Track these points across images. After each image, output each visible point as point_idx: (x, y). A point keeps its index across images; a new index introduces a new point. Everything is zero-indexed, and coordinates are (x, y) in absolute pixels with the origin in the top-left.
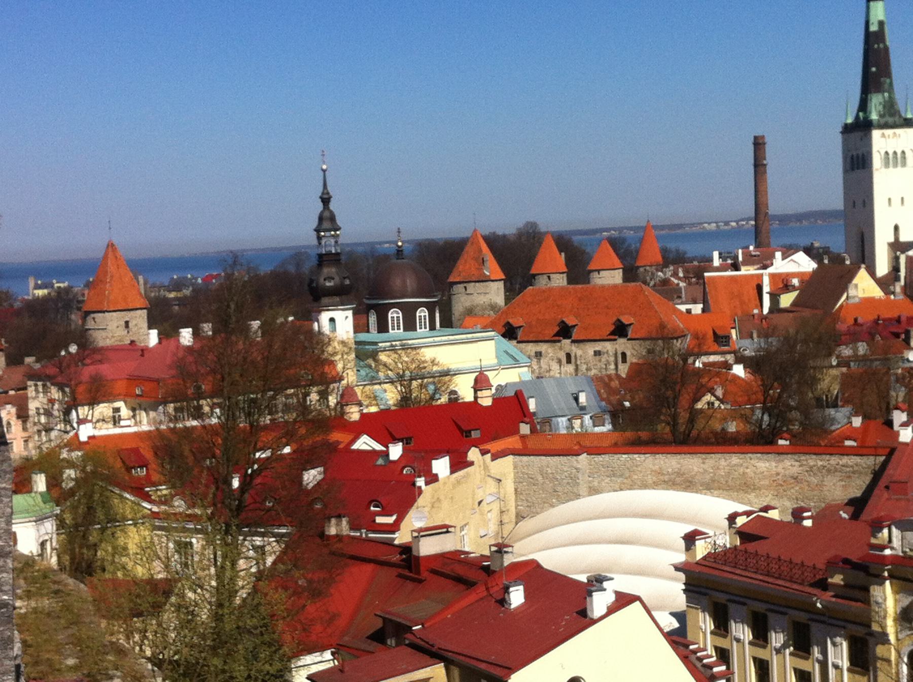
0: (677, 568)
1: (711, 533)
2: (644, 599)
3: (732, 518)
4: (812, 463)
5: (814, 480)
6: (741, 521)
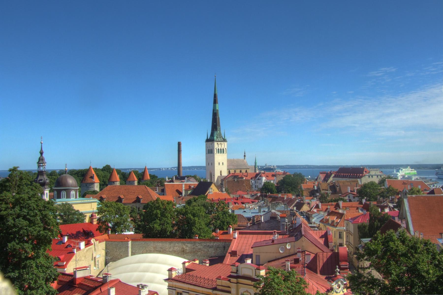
0: (166, 280)
1: (177, 269)
2: (158, 293)
3: (184, 263)
4: (205, 244)
5: (206, 250)
6: (187, 264)
